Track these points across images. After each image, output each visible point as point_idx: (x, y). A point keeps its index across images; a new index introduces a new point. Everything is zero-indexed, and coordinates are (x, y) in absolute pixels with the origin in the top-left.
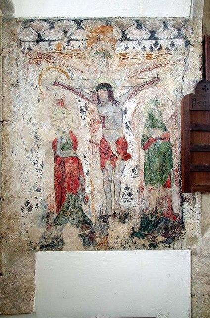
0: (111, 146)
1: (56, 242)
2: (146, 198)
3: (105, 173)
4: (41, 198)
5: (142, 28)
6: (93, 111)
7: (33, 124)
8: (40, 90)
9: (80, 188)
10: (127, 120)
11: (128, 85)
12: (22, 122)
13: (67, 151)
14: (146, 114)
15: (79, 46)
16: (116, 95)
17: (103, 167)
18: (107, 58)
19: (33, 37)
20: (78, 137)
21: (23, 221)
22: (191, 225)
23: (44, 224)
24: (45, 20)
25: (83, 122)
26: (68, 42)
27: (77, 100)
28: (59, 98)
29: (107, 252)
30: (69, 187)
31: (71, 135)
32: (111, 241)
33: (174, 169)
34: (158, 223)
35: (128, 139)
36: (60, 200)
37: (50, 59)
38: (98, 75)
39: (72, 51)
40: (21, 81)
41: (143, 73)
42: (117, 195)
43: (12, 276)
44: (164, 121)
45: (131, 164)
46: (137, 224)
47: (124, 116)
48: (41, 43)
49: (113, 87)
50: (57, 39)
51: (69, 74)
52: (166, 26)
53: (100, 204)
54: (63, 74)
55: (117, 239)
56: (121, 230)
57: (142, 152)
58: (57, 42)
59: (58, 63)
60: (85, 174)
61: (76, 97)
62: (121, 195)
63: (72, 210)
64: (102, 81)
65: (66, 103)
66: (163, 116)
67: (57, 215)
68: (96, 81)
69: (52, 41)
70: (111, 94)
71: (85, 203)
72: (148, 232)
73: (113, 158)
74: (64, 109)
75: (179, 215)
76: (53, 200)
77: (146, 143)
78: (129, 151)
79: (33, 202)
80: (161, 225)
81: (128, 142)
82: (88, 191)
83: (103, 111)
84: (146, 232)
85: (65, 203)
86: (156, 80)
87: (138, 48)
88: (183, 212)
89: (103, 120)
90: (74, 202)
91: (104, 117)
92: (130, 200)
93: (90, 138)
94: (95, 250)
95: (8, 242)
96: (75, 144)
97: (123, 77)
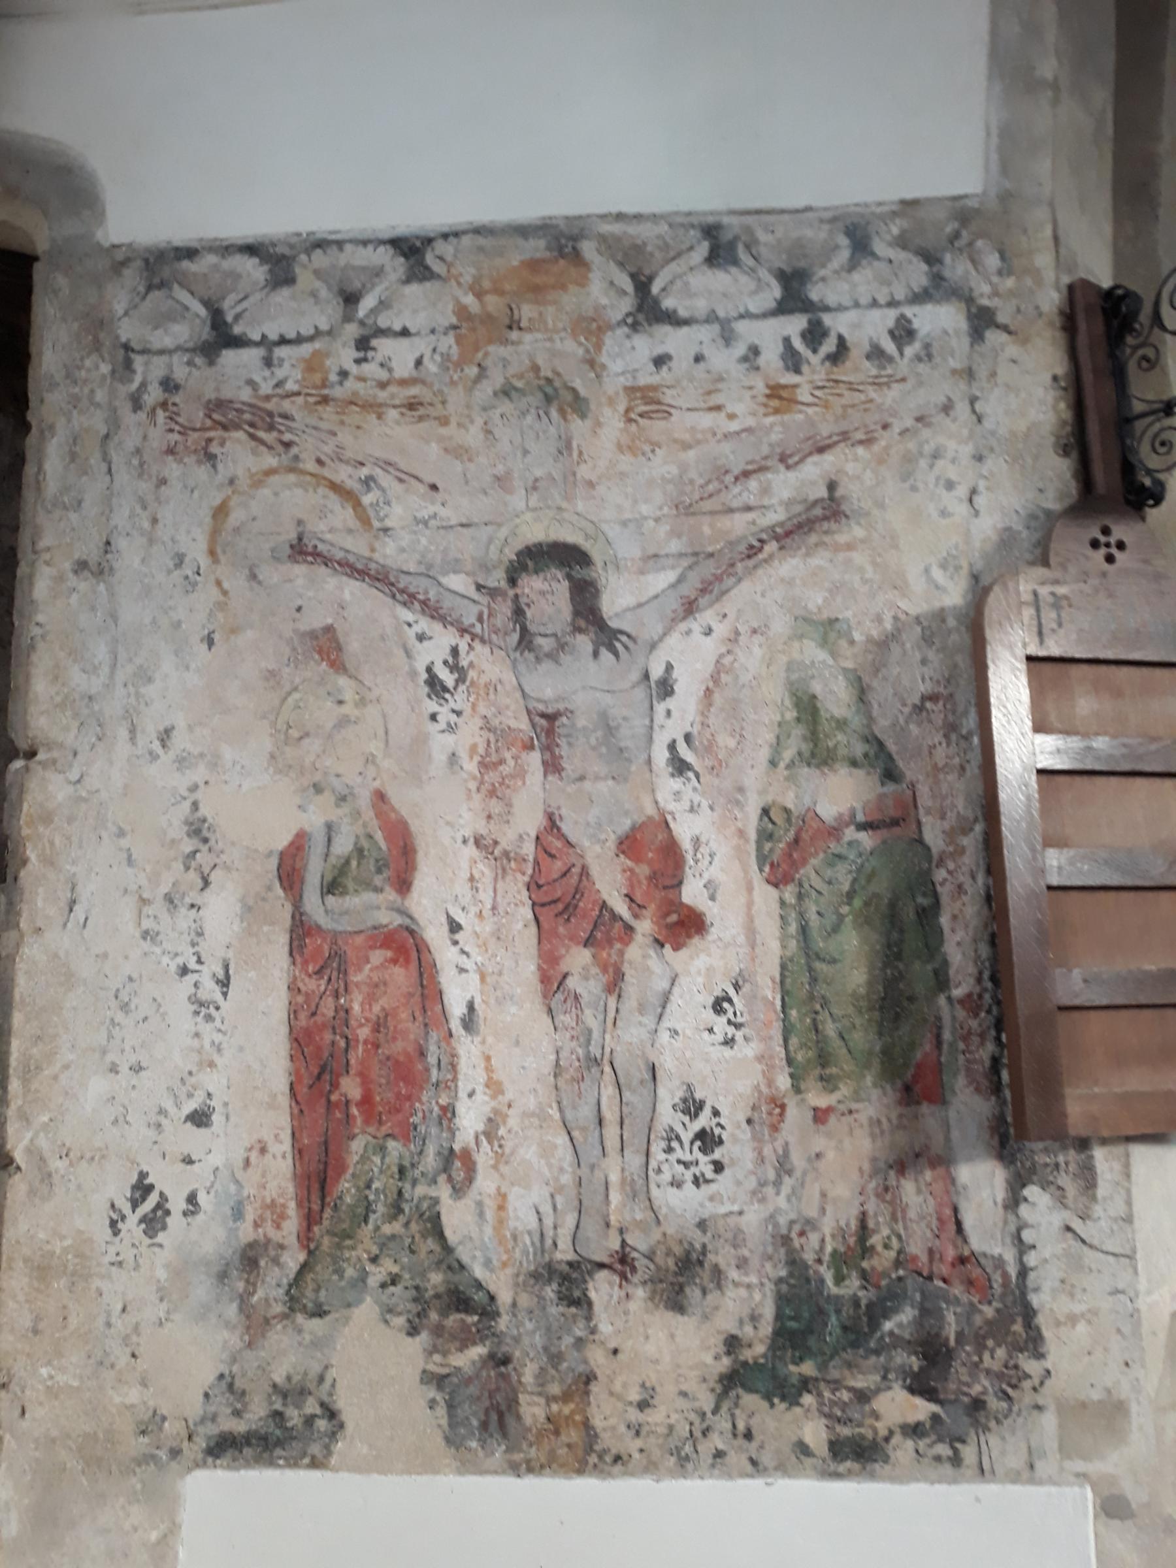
0: (595, 871)
1: (294, 1417)
2: (798, 1160)
4: (216, 1159)
5: (735, 262)
6: (492, 687)
7: (182, 762)
8: (219, 583)
9: (429, 1101)
11: (674, 546)
12: (123, 748)
13: (353, 901)
14: (775, 692)
15: (419, 362)
16: (618, 599)
17: (552, 982)
18: (562, 412)
20: (415, 826)
21: (116, 1288)
22: (1081, 1327)
24: (251, 249)
25: (441, 744)
26: (363, 344)
27: (411, 633)
28: (316, 619)
30: (366, 1101)
31: (378, 815)
32: (606, 1414)
33: (957, 993)
34: (877, 1312)
35: (684, 830)
36: (318, 1174)
37: (271, 428)
38: (517, 501)
39: (383, 385)
40: (121, 543)
41: (753, 484)
42: (635, 1142)
44: (882, 726)
45: (701, 968)
46: (754, 1318)
47: (660, 708)
48: (229, 357)
50: (307, 331)
51: (367, 499)
53: (538, 1194)
54: (333, 500)
55: (643, 1405)
56: (659, 1351)
57: (766, 898)
58: (306, 349)
59: (308, 448)
60: (455, 1025)
61: (406, 615)
62: (657, 1148)
63: (387, 1229)
64: (536, 532)
65: (353, 646)
66: (873, 699)
67: (302, 1257)
68: (503, 532)
69: (283, 341)
71: (458, 1191)
72: (823, 1367)
73: (605, 932)
74: (343, 681)
75: (999, 1263)
76: (278, 1174)
77: (785, 848)
78: (692, 893)
79: (171, 1184)
80: (899, 1322)
81: (686, 845)
82: (470, 1120)
84: (808, 1368)
85: (346, 1189)
86: (825, 513)
88: (1022, 1247)
89: (550, 732)
90: (393, 1184)
91: (551, 718)
93: (482, 827)
94: (515, 1469)
95: (34, 1412)
96: (398, 860)
97: (645, 509)
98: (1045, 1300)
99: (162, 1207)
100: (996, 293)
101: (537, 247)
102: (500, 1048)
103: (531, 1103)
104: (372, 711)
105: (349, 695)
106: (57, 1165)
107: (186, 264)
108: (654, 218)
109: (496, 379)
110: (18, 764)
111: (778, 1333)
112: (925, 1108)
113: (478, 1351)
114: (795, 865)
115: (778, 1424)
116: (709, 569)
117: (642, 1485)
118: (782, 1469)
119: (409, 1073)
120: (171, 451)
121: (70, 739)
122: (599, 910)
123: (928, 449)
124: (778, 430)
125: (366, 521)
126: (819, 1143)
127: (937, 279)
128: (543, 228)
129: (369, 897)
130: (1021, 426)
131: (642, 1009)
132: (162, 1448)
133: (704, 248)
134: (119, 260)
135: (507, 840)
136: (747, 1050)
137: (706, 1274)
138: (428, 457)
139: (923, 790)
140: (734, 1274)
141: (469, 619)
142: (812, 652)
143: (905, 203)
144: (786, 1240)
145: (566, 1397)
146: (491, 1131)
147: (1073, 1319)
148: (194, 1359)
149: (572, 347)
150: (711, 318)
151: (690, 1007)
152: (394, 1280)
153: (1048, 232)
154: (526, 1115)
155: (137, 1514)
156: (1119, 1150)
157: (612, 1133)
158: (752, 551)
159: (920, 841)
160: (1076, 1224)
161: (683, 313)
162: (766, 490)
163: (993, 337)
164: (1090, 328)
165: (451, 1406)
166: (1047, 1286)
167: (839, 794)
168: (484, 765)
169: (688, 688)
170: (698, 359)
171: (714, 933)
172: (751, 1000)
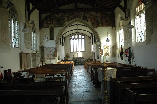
102: (50, 56)
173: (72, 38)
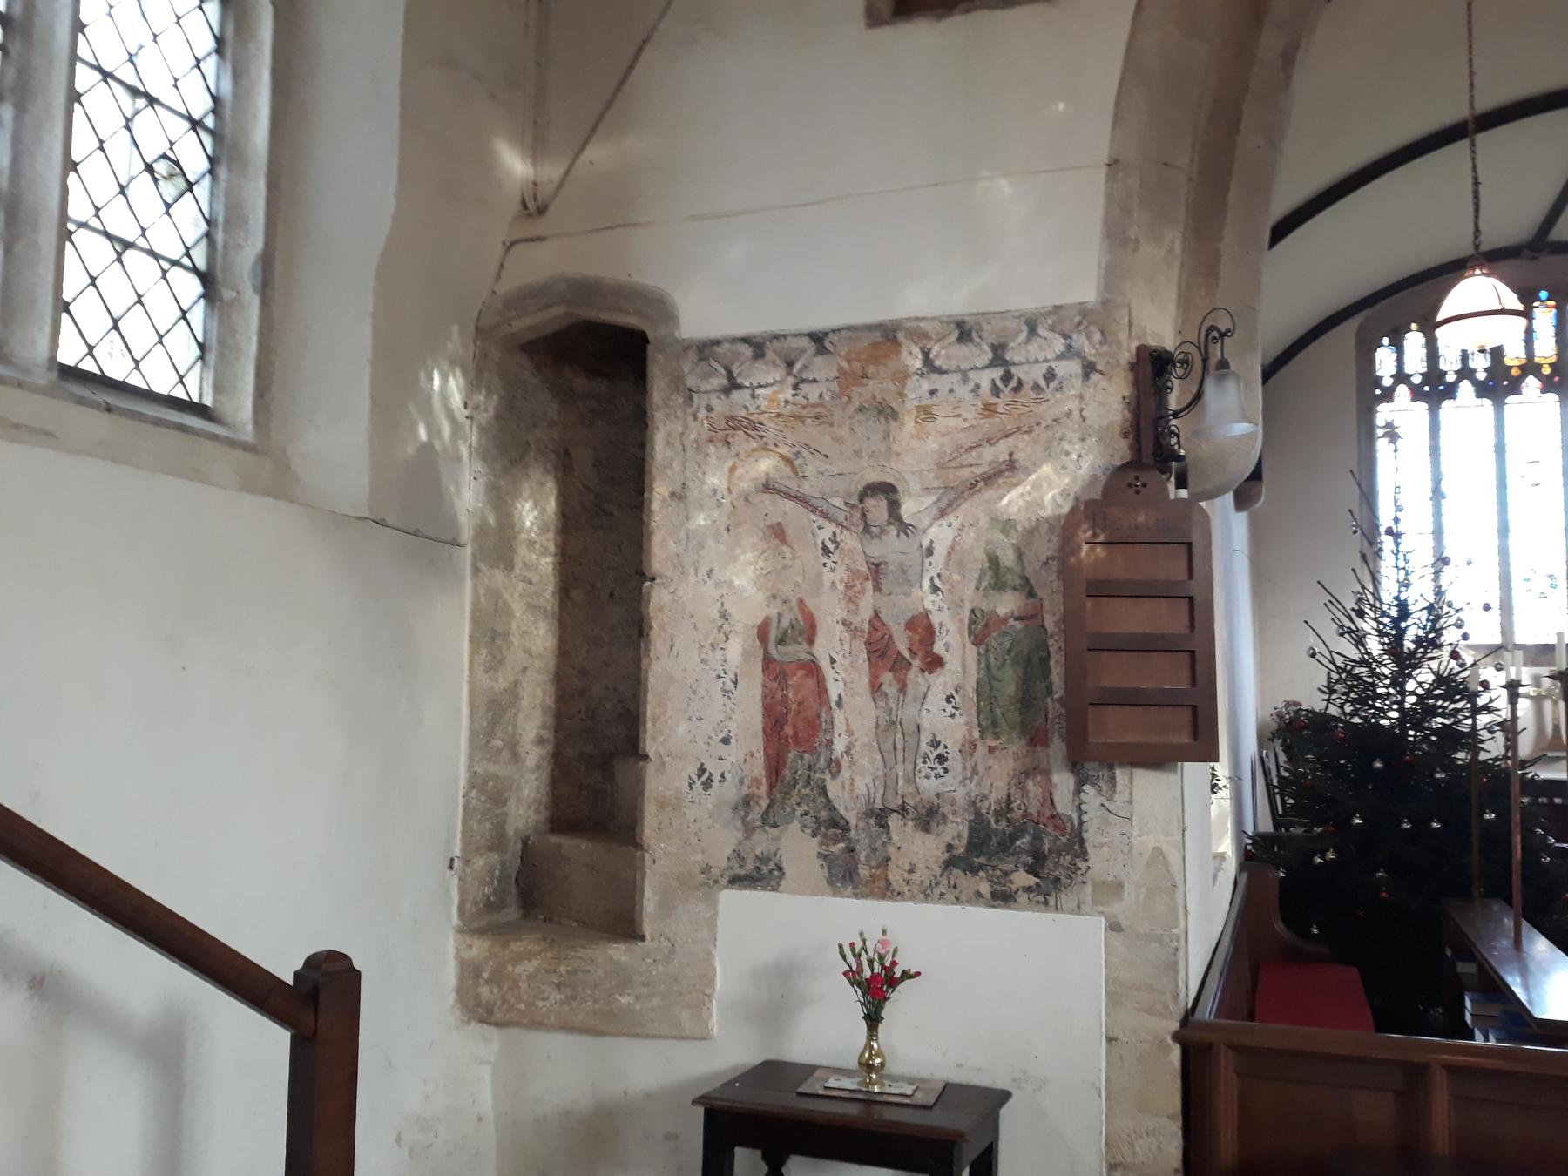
0: (895, 637)
1: (765, 870)
2: (981, 768)
3: (882, 704)
4: (732, 759)
5: (971, 340)
7: (717, 585)
9: (822, 738)
10: (932, 572)
11: (936, 484)
12: (692, 579)
13: (792, 648)
14: (980, 555)
16: (908, 509)
17: (876, 687)
19: (719, 381)
20: (816, 613)
21: (691, 813)
22: (1105, 849)
23: (739, 823)
24: (745, 340)
25: (828, 577)
28: (773, 520)
29: (886, 904)
30: (795, 736)
32: (896, 875)
33: (1056, 696)
34: (1014, 837)
35: (935, 620)
36: (775, 767)
39: (804, 407)
40: (690, 484)
41: (974, 453)
42: (910, 759)
43: (665, 944)
44: (1029, 571)
45: (941, 682)
46: (959, 836)
47: (927, 561)
48: (736, 395)
49: (900, 489)
51: (797, 463)
52: (1033, 331)
53: (868, 779)
55: (911, 871)
56: (919, 850)
60: (833, 705)
61: (814, 517)
62: (920, 761)
64: (873, 476)
65: (790, 532)
66: (1025, 558)
69: (760, 386)
70: (894, 506)
71: (834, 776)
72: (989, 859)
73: (899, 665)
74: (785, 548)
75: (1070, 818)
76: (758, 767)
77: (981, 629)
78: (938, 648)
79: (714, 769)
80: (1023, 842)
81: (936, 626)
82: (839, 746)
83: (876, 550)
84: (982, 860)
85: (787, 772)
87: (963, 391)
88: (1081, 813)
89: (877, 572)
91: (877, 565)
92: (941, 772)
94: (856, 896)
95: (660, 862)
96: (809, 630)
97: (923, 466)
98: (1090, 836)
99: (710, 779)
100: (1097, 354)
101: (877, 336)
102: (853, 715)
103: (866, 740)
104: (798, 562)
105: (788, 555)
106: (666, 759)
107: (717, 349)
108: (933, 319)
109: (856, 403)
110: (648, 584)
111: (969, 843)
112: (1039, 748)
113: (841, 845)
114: (985, 636)
115: (966, 882)
116: (952, 495)
117: (910, 905)
118: (969, 902)
119: (813, 725)
120: (711, 441)
121: (669, 574)
122: (897, 654)
123: (1058, 435)
124: (987, 425)
125: (796, 473)
126: (991, 762)
127: (1069, 347)
128: (880, 326)
129: (795, 647)
130: (1105, 423)
131: (915, 700)
132: (709, 882)
133: (956, 334)
134: (687, 346)
135: (856, 622)
136: (960, 720)
137: (939, 816)
138: (824, 441)
139: (1046, 603)
140: (951, 817)
141: (841, 519)
142: (997, 535)
143: (1056, 307)
144: (974, 803)
145: (878, 867)
146: (848, 751)
147: (1102, 845)
148: (722, 842)
149: (890, 386)
150: (958, 370)
151: (936, 700)
152: (806, 813)
153: (1126, 321)
154: (863, 745)
155: (701, 906)
156: (1128, 770)
157: (900, 758)
158: (973, 486)
159: (1043, 626)
160: (1106, 803)
161: (945, 368)
162: (980, 456)
163: (1095, 377)
164: (1149, 370)
165: (830, 869)
166: (1092, 829)
167: (1007, 604)
168: (848, 587)
169: (940, 551)
170: (951, 391)
171: (948, 666)
172: (963, 697)
173: (1401, 377)
